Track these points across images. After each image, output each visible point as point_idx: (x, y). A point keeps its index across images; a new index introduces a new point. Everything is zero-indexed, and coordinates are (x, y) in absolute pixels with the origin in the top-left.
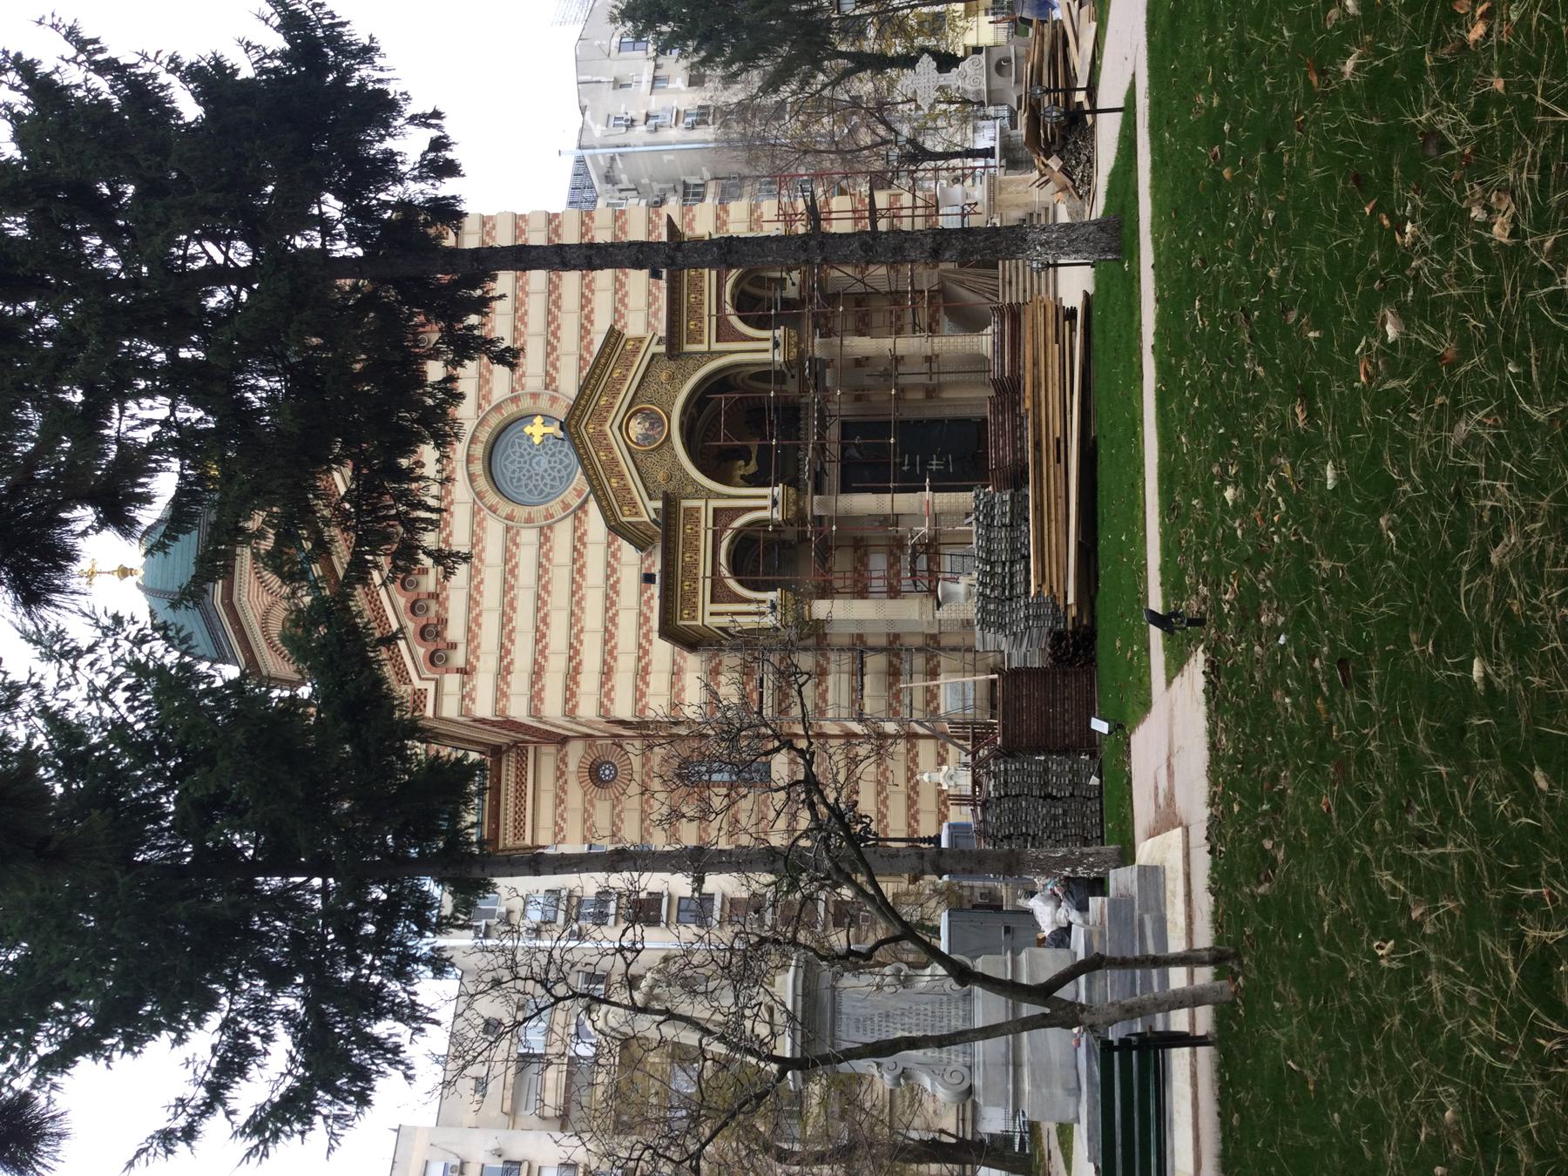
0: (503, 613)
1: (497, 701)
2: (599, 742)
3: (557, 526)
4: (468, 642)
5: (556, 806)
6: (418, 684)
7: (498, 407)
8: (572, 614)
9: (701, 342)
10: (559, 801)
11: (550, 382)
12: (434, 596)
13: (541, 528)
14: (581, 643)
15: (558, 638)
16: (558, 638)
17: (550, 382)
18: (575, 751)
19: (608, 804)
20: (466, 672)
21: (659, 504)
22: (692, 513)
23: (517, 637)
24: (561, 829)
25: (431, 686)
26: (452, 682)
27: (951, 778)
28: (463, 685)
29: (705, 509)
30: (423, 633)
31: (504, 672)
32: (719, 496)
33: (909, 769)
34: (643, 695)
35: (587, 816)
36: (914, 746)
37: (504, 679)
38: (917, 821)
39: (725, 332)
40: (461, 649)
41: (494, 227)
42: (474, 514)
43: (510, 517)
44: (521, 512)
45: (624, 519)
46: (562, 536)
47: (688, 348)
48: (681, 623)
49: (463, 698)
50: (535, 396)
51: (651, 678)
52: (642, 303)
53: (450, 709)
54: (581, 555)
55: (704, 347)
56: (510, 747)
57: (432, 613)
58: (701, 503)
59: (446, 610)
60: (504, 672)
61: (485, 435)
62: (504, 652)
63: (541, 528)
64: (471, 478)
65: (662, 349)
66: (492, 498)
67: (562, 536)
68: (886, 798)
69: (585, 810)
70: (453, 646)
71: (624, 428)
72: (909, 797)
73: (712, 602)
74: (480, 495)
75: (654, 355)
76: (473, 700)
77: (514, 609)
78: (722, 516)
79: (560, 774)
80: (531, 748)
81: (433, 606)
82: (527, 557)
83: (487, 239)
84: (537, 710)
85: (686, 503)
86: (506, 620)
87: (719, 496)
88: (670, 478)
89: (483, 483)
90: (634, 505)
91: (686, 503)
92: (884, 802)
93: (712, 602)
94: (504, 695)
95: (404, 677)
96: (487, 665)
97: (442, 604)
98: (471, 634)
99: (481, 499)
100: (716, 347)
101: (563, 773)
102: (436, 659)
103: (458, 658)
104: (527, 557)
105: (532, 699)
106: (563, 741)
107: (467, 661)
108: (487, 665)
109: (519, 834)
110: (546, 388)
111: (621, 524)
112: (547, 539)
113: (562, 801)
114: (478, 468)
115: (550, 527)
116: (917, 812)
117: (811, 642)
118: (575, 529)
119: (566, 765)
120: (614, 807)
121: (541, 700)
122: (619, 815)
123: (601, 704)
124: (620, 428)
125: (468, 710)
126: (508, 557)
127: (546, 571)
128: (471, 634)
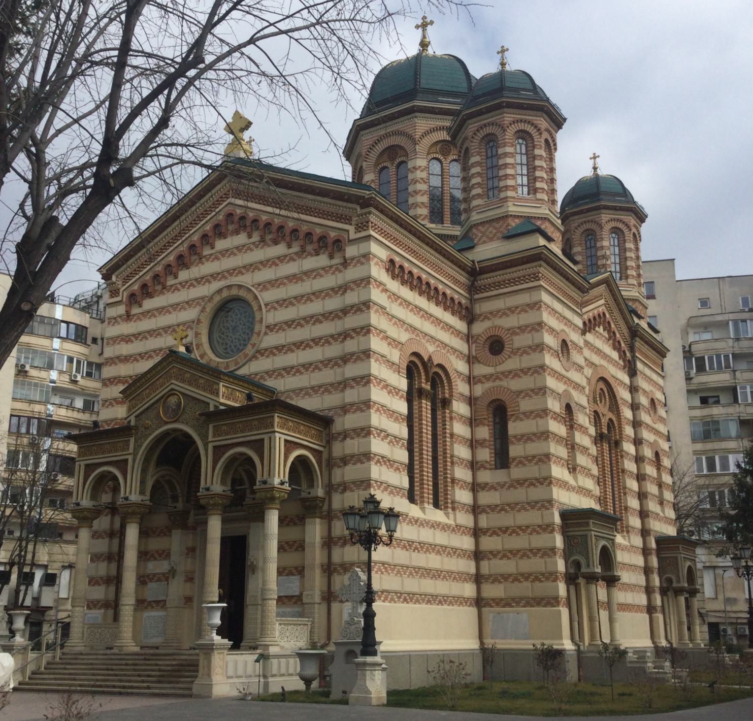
4: (142, 313)
7: (256, 298)
9: (214, 436)
11: (270, 328)
12: (164, 288)
17: (270, 328)
20: (128, 317)
21: (133, 423)
26: (121, 310)
28: (120, 317)
31: (127, 339)
32: (134, 461)
37: (123, 340)
39: (219, 451)
41: (362, 264)
42: (202, 298)
47: (211, 426)
49: (115, 318)
50: (261, 320)
52: (314, 383)
55: (210, 439)
58: (131, 450)
60: (127, 339)
64: (220, 291)
65: (212, 409)
66: (210, 308)
70: (140, 306)
71: (172, 393)
73: (87, 466)
75: (208, 404)
81: (159, 287)
83: (376, 260)
85: (132, 440)
87: (134, 461)
88: (146, 428)
89: (217, 299)
91: (132, 440)
93: (87, 466)
95: (125, 281)
97: (162, 293)
99: (209, 301)
100: (210, 446)
103: (135, 310)
107: (134, 315)
110: (267, 327)
124: (172, 389)
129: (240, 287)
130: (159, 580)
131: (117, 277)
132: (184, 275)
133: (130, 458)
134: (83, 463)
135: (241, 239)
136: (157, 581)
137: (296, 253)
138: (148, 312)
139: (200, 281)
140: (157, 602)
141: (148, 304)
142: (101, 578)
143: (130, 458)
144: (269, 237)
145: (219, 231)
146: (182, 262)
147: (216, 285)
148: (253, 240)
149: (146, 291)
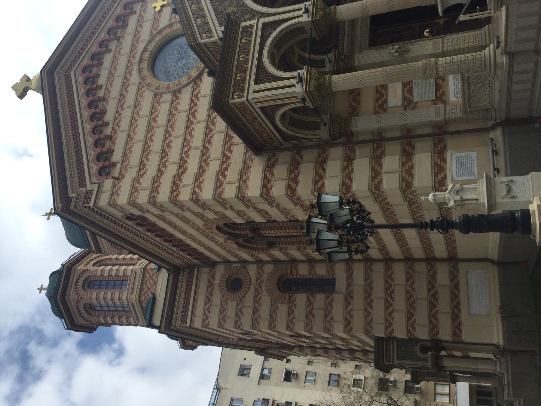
0: (146, 143)
1: (131, 194)
2: (234, 265)
3: (184, 90)
5: (206, 304)
6: (89, 187)
7: (161, 31)
8: (185, 139)
10: (208, 300)
13: (175, 92)
14: (188, 156)
15: (174, 155)
16: (174, 155)
18: (220, 270)
19: (234, 303)
22: (248, 30)
23: (151, 157)
24: (207, 318)
25: (95, 188)
27: (457, 193)
28: (114, 186)
29: (256, 24)
30: (98, 158)
33: (429, 283)
34: (221, 184)
35: (222, 311)
36: (433, 267)
38: (437, 319)
40: (118, 166)
42: (138, 90)
43: (158, 88)
44: (164, 84)
45: (201, 41)
46: (185, 97)
48: (231, 101)
49: (112, 194)
51: (228, 174)
53: (103, 201)
54: (195, 104)
56: (184, 268)
57: (107, 146)
59: (114, 144)
61: (151, 48)
62: (142, 165)
63: (175, 92)
64: (140, 70)
66: (150, 79)
67: (185, 97)
68: (414, 302)
69: (222, 306)
70: (114, 165)
72: (430, 302)
74: (143, 79)
76: (118, 195)
77: (152, 140)
78: (267, 28)
79: (210, 284)
80: (196, 270)
81: (108, 144)
82: (163, 110)
84: (155, 198)
86: (146, 147)
90: (210, 31)
91: (243, 24)
92: (412, 305)
93: (256, 83)
94: (137, 190)
95: (82, 183)
96: (131, 174)
97: (113, 142)
98: (125, 156)
101: (212, 284)
102: (104, 172)
103: (116, 172)
104: (163, 110)
105: (152, 192)
106: (213, 264)
107: (121, 173)
108: (131, 174)
109: (184, 321)
111: (199, 45)
112: (177, 98)
113: (209, 301)
114: (145, 65)
115: (179, 91)
116: (437, 313)
117: (343, 140)
118: (194, 90)
119: (214, 279)
120: (238, 305)
121: (158, 192)
122: (241, 310)
123: (194, 192)
125: (114, 201)
126: (153, 110)
127: (174, 116)
128: (125, 156)
129: (145, 50)
130: (411, 92)
131: (73, 193)
132: (109, 117)
133: (263, 20)
134: (253, 87)
135: (108, 59)
136: (412, 94)
137: (142, 7)
138: (125, 154)
139: (122, 96)
140: (438, 87)
141: (117, 157)
142: (403, 164)
143: (263, 20)
144: (119, 34)
145: (91, 80)
146: (98, 116)
147: (135, 78)
148: (113, 50)
149: (104, 157)
